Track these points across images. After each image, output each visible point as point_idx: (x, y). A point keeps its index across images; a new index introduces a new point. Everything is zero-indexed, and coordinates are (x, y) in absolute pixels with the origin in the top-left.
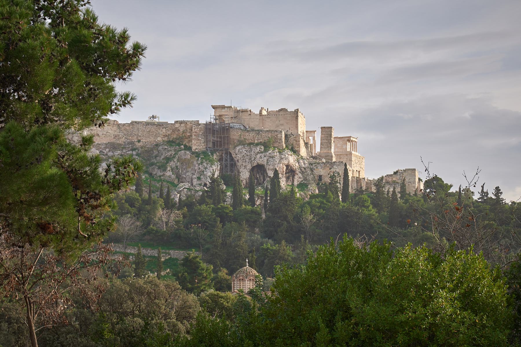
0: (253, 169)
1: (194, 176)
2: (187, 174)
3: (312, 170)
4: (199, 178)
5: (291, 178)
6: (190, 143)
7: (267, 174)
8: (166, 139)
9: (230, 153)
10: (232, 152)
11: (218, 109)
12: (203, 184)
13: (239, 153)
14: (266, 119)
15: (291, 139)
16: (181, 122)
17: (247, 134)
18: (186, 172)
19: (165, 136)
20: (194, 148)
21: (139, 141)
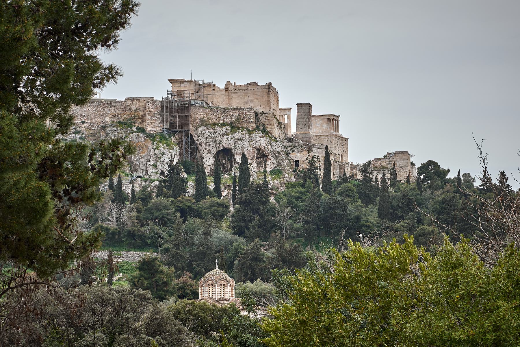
0: (218, 153)
1: (149, 163)
2: (141, 160)
3: (287, 154)
4: (155, 166)
5: (263, 164)
6: (144, 124)
7: (235, 159)
8: (115, 119)
9: (191, 135)
10: (194, 134)
11: (176, 83)
12: (159, 172)
13: (202, 135)
14: (233, 95)
15: (262, 119)
16: (133, 100)
17: (211, 112)
18: (139, 158)
19: (114, 116)
20: (148, 130)
21: (83, 123)
